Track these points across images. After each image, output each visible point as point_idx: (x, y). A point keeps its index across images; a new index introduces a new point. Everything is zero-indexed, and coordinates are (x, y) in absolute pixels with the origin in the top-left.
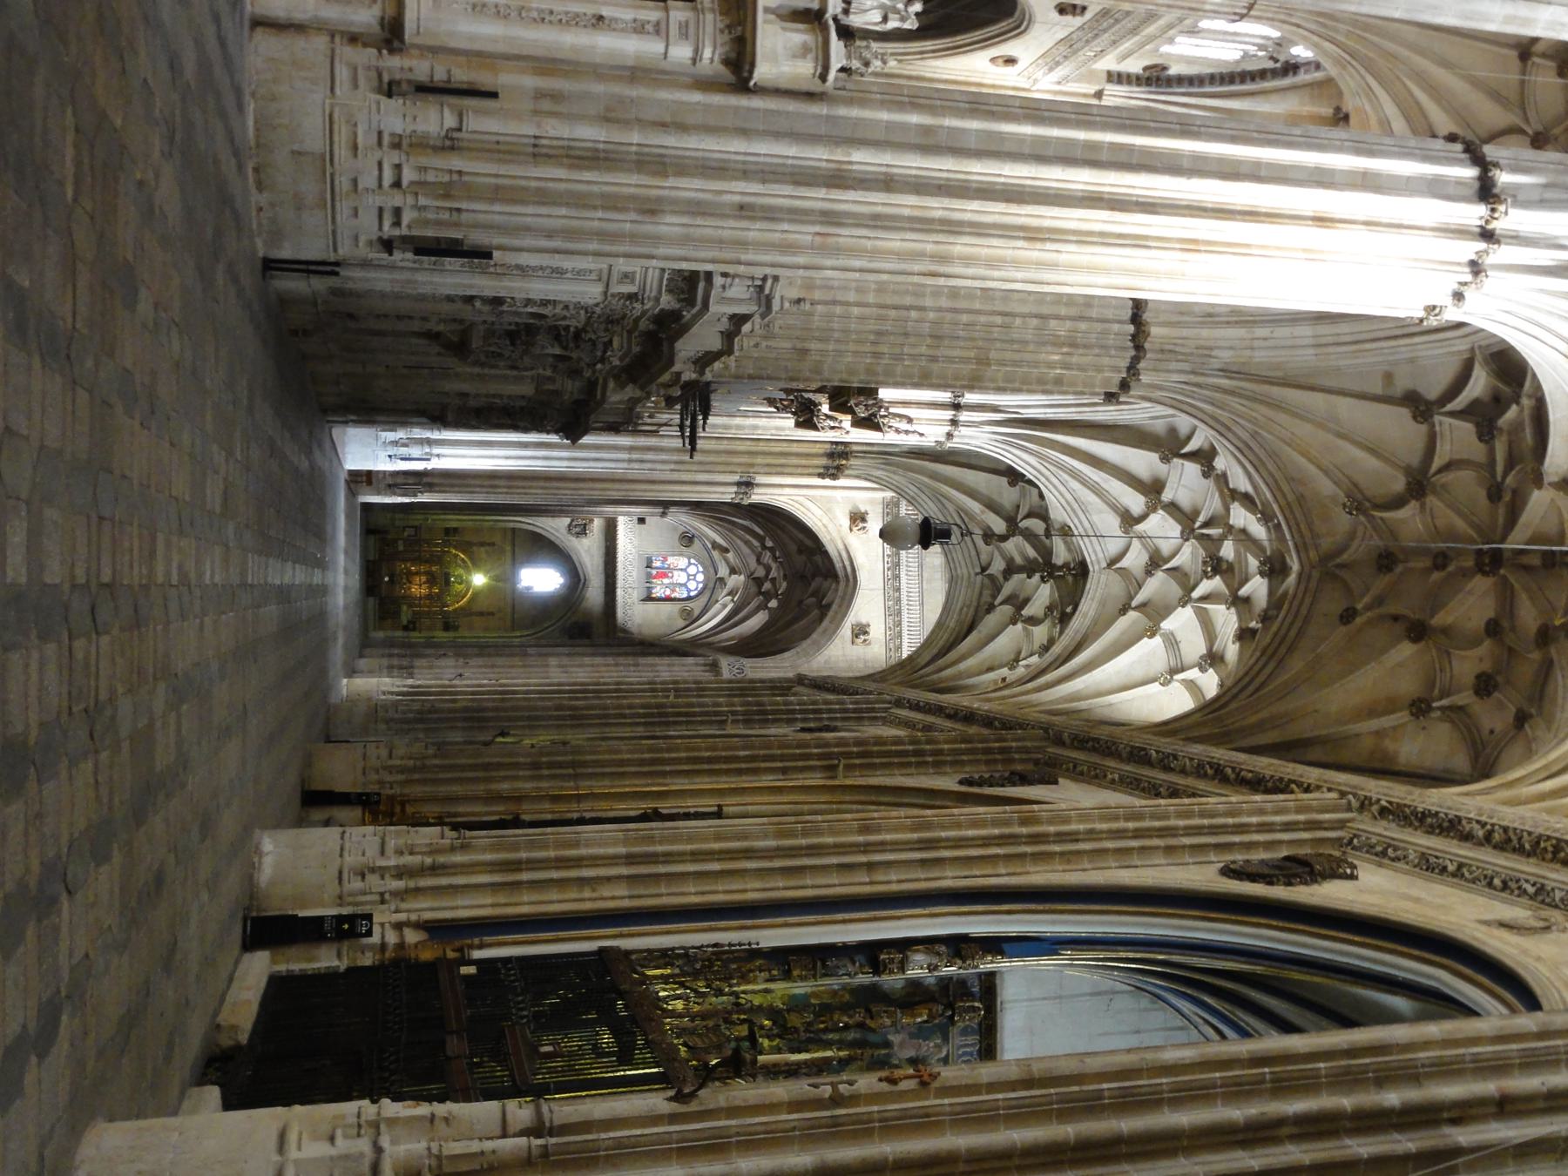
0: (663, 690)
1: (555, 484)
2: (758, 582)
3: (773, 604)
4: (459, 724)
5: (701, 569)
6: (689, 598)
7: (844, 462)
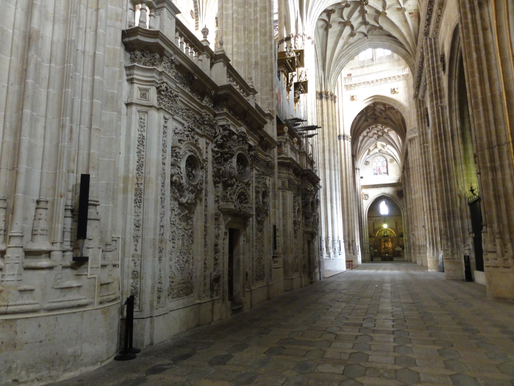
0: (424, 148)
1: (349, 200)
2: (379, 137)
3: (386, 130)
4: (452, 222)
5: (376, 158)
6: (386, 161)
7: (329, 93)
